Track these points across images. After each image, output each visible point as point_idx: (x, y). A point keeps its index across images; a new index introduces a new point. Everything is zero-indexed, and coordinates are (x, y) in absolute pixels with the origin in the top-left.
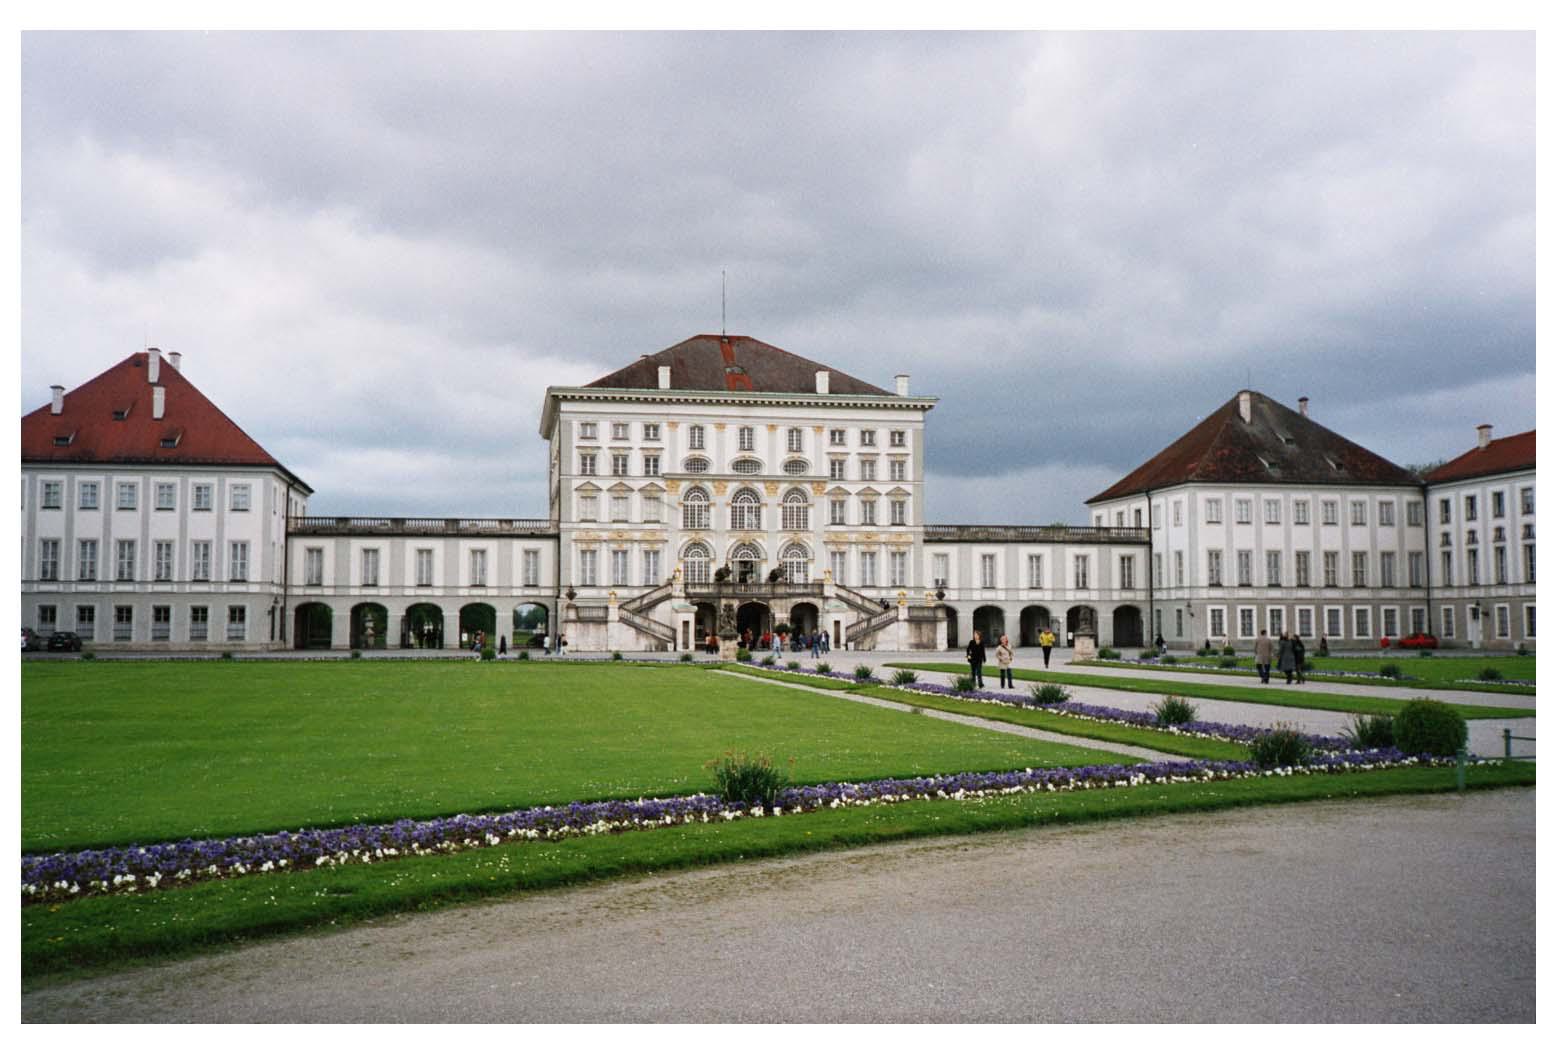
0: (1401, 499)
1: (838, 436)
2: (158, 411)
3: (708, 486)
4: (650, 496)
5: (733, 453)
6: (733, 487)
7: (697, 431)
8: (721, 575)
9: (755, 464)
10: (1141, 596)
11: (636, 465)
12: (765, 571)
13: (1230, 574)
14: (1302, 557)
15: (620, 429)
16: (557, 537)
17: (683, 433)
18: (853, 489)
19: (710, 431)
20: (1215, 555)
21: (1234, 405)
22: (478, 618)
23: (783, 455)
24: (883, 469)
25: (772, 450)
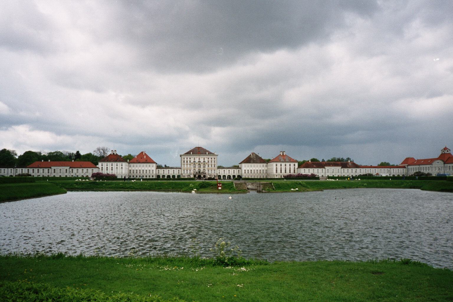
0: (265, 164)
1: (208, 159)
2: (145, 158)
3: (196, 164)
4: (190, 165)
5: (198, 160)
6: (198, 164)
7: (194, 158)
8: (197, 172)
9: (200, 162)
10: (240, 174)
11: (189, 162)
12: (201, 172)
13: (247, 172)
14: (254, 170)
15: (187, 158)
16: (181, 169)
17: (193, 159)
18: (210, 164)
19: (196, 158)
20: (245, 170)
21: (250, 155)
22: (174, 176)
23: (203, 160)
24: (213, 162)
25: (202, 160)
